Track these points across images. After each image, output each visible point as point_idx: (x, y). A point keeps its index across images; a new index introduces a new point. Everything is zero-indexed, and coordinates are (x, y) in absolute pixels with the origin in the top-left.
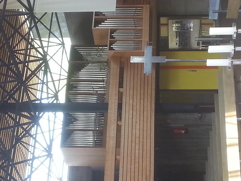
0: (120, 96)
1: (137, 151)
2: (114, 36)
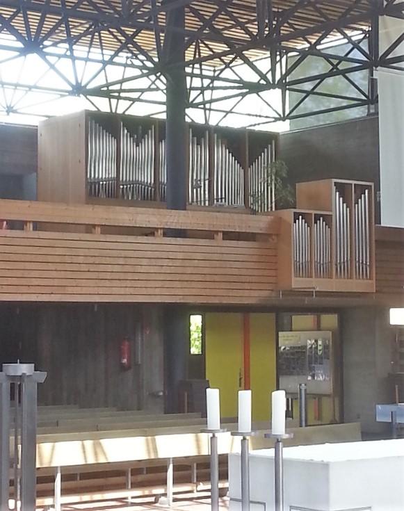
0: (210, 235)
1: (109, 268)
2: (318, 222)
